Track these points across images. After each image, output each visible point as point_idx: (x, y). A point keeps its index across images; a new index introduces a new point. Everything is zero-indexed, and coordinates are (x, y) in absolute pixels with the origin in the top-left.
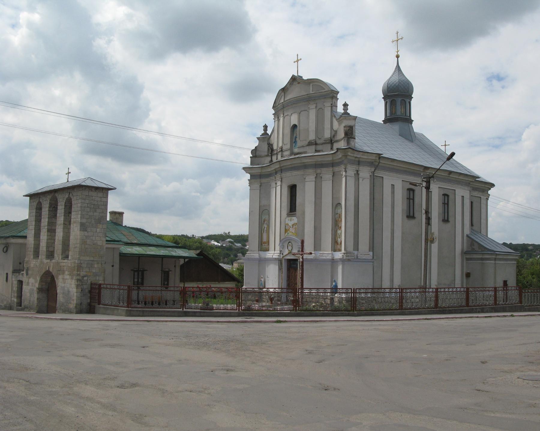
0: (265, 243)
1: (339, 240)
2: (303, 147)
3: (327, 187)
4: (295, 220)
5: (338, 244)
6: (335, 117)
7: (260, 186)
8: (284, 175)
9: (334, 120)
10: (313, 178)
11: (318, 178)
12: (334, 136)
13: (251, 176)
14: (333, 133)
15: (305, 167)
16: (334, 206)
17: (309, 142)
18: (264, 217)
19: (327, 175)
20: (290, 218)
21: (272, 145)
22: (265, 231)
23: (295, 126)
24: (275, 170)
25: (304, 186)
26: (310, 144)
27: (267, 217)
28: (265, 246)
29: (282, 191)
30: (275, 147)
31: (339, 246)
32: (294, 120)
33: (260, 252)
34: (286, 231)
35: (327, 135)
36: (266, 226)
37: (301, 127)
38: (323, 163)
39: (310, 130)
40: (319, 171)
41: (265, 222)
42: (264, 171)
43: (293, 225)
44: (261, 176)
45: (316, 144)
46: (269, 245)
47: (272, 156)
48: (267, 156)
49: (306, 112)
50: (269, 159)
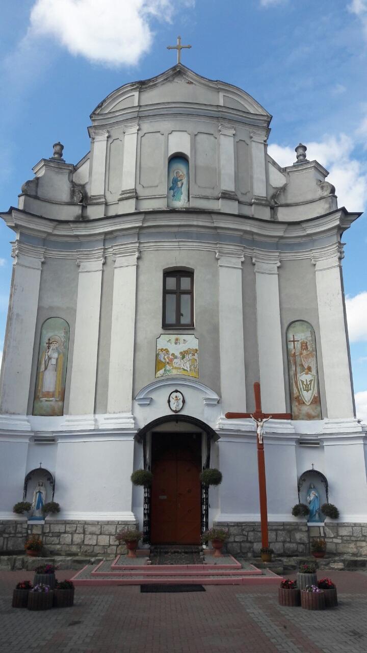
0: (48, 394)
1: (307, 396)
2: (207, 198)
3: (268, 287)
4: (190, 341)
5: (301, 403)
6: (274, 163)
7: (43, 263)
8: (149, 245)
9: (272, 169)
10: (237, 262)
11: (248, 266)
12: (274, 196)
13: (21, 234)
14: (271, 192)
15: (217, 235)
16: (286, 326)
17: (223, 193)
18: (47, 335)
19: (268, 264)
20: (173, 337)
21: (83, 186)
22: (50, 367)
23: (178, 157)
24: (106, 234)
25: (215, 275)
26: (226, 196)
27: (61, 334)
28: (45, 403)
29: (142, 278)
30: (95, 189)
31: (305, 409)
32: (180, 143)
33: (31, 417)
34: (159, 364)
35: (260, 190)
36: (55, 355)
37: (200, 161)
38: (256, 237)
39: (223, 172)
40: (249, 252)
41: (52, 347)
42: (62, 231)
43: (183, 355)
44: (46, 241)
45: (240, 202)
46: (63, 399)
47: (84, 208)
48: (71, 203)
49: (212, 138)
50: (76, 211)
